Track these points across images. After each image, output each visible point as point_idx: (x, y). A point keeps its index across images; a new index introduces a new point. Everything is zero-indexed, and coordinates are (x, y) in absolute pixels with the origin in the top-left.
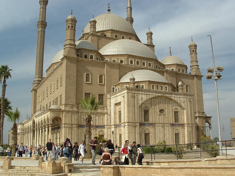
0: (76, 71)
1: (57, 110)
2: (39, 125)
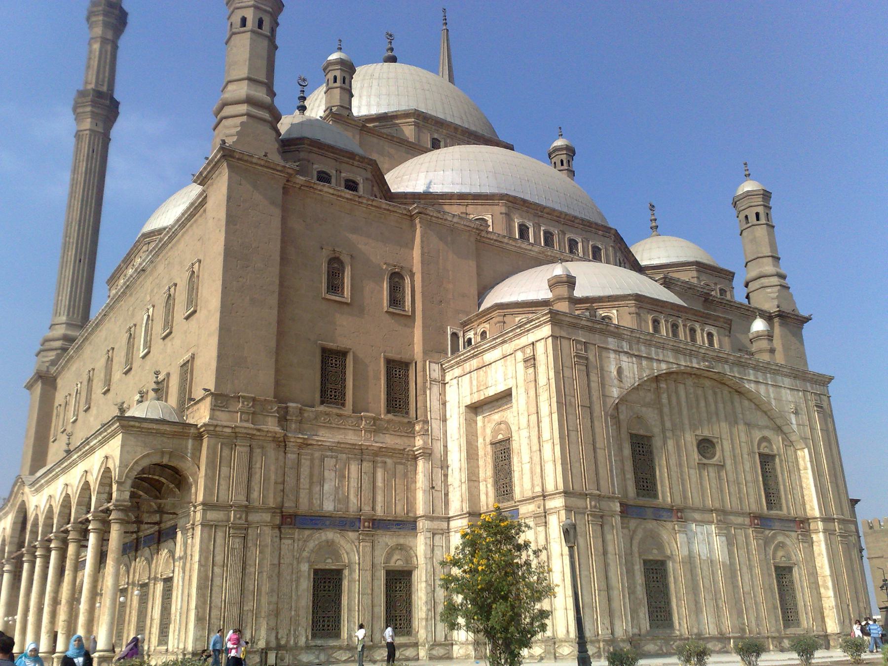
0: (279, 232)
1: (167, 428)
2: (48, 525)
